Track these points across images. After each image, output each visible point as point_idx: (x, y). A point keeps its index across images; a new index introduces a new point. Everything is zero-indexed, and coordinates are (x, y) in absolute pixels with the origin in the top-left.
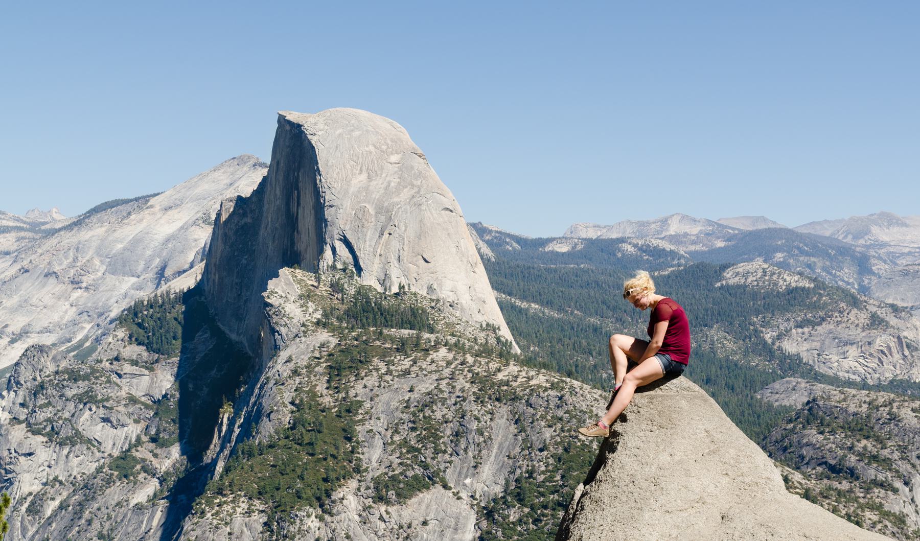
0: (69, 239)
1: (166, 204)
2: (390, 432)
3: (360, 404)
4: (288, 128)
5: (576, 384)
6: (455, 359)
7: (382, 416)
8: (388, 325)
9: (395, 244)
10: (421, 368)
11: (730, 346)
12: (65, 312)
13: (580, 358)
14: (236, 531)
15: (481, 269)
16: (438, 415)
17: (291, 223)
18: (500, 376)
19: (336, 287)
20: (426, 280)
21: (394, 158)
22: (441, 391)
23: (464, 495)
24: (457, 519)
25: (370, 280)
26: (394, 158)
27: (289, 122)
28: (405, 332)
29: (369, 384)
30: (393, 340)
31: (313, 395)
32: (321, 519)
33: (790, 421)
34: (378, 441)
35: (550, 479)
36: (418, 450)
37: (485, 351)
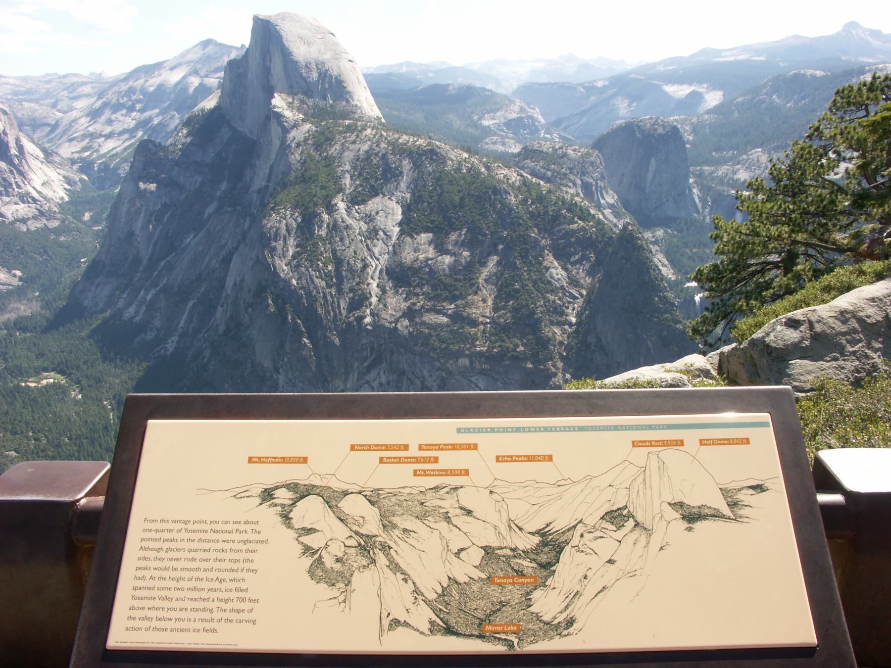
1: (172, 65)
2: (352, 171)
3: (335, 157)
4: (260, 22)
5: (437, 143)
6: (376, 134)
7: (347, 164)
10: (361, 140)
11: (458, 123)
14: (289, 221)
16: (375, 161)
18: (400, 141)
19: (302, 102)
21: (319, 36)
22: (374, 150)
23: (393, 198)
24: (393, 210)
27: (260, 19)
28: (347, 122)
29: (338, 148)
32: (329, 214)
33: (516, 157)
34: (348, 176)
35: (434, 189)
36: (368, 178)
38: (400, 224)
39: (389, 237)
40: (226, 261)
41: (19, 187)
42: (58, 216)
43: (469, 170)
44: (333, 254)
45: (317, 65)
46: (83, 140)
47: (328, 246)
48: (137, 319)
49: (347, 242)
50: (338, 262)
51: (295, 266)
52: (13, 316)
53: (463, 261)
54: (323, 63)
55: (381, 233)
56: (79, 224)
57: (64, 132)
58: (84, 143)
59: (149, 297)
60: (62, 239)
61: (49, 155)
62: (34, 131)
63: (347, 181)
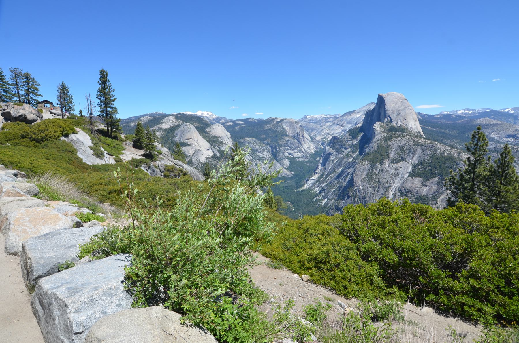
0: (341, 119)
3: (390, 146)
5: (436, 143)
8: (396, 132)
9: (399, 117)
12: (340, 130)
13: (438, 138)
15: (418, 121)
17: (379, 114)
20: (406, 123)
21: (401, 101)
24: (408, 167)
25: (394, 124)
26: (401, 101)
28: (400, 133)
30: (397, 134)
31: (381, 144)
34: (393, 153)
35: (429, 161)
37: (417, 136)
38: (410, 173)
39: (402, 177)
40: (346, 178)
41: (299, 148)
42: (309, 158)
43: (448, 154)
44: (379, 180)
45: (396, 111)
46: (324, 135)
47: (377, 177)
48: (318, 192)
49: (385, 176)
50: (379, 182)
51: (363, 182)
52: (287, 185)
53: (432, 191)
54: (399, 111)
55: (400, 176)
56: (315, 161)
57: (320, 132)
58: (324, 136)
59: (323, 186)
60: (308, 165)
61: (312, 139)
62: (312, 132)
63: (392, 155)
